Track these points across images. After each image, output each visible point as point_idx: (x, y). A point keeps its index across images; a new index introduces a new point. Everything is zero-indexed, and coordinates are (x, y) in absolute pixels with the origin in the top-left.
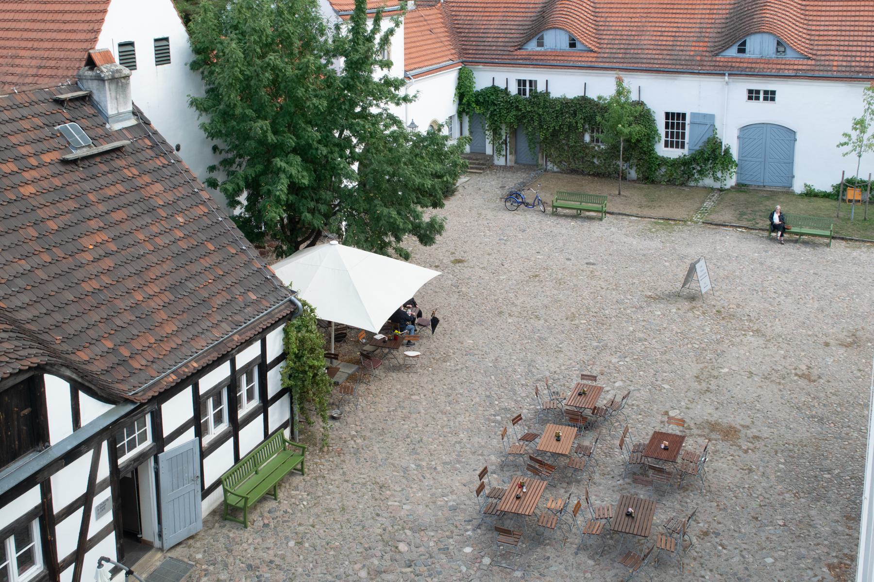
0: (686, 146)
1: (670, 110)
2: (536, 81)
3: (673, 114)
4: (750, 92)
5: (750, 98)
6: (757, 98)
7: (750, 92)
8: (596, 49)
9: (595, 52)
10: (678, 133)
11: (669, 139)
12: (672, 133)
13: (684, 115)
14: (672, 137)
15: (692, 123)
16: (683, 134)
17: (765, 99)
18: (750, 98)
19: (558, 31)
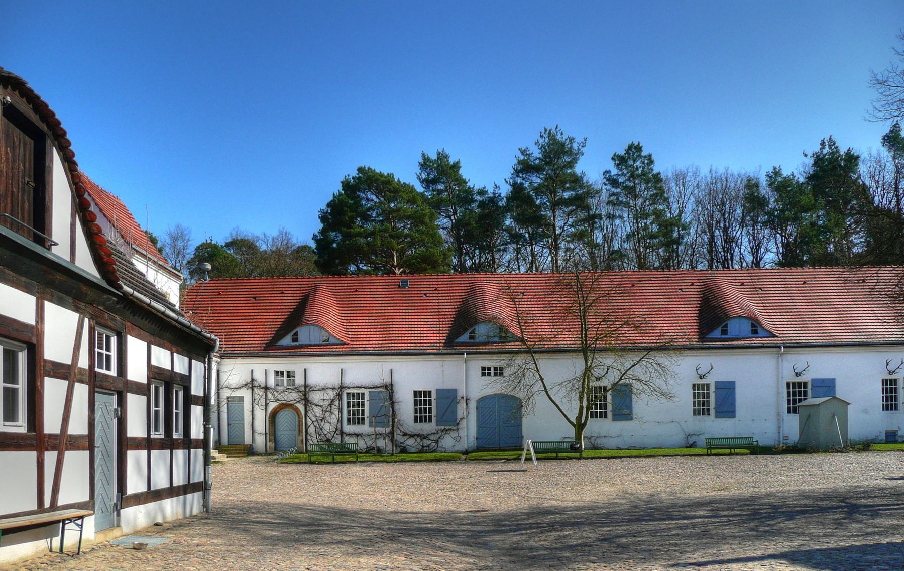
0: (434, 419)
1: (418, 389)
2: (294, 372)
3: (420, 392)
4: (483, 369)
5: (483, 374)
6: (489, 374)
7: (483, 369)
8: (348, 342)
9: (347, 344)
10: (425, 409)
11: (418, 415)
12: (421, 409)
13: (430, 392)
14: (421, 413)
15: (437, 398)
16: (430, 409)
17: (495, 374)
18: (483, 374)
19: (312, 327)
